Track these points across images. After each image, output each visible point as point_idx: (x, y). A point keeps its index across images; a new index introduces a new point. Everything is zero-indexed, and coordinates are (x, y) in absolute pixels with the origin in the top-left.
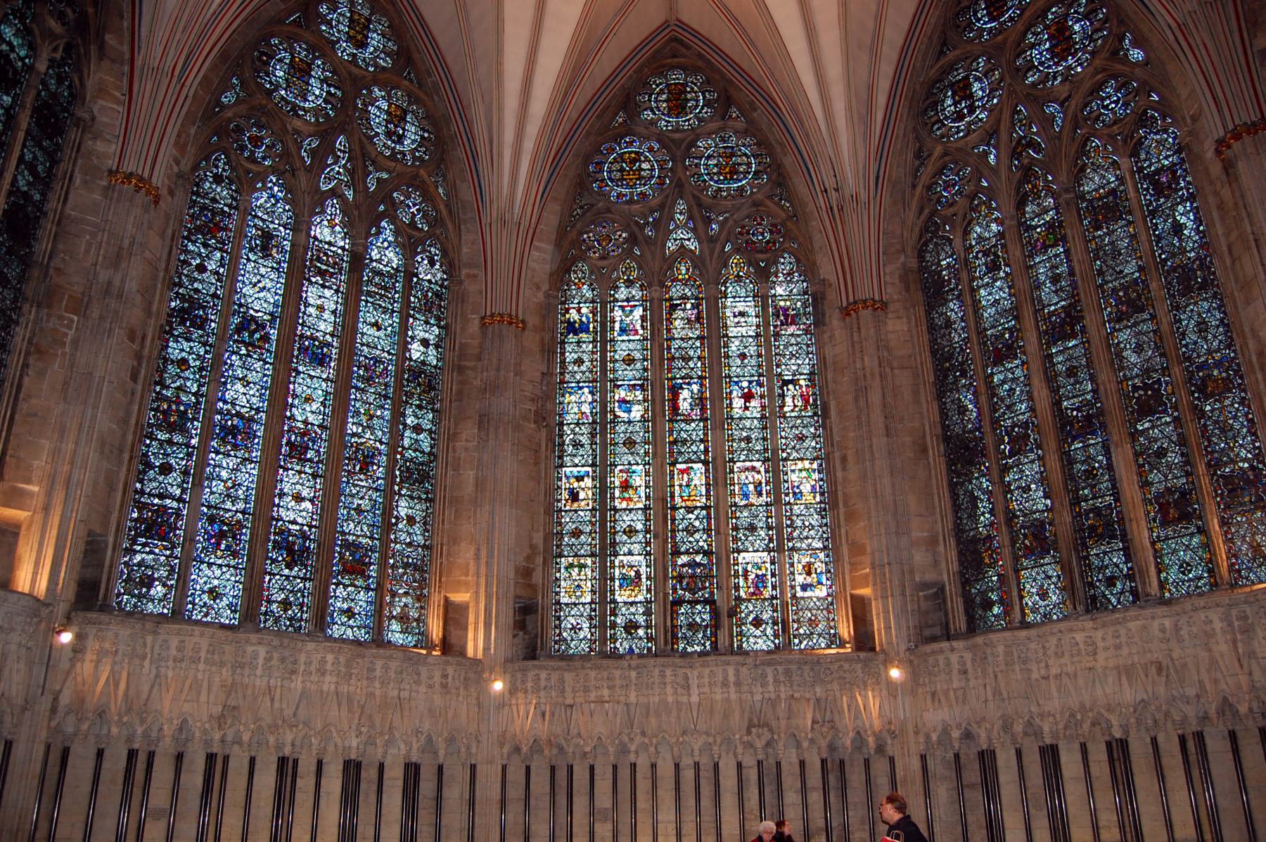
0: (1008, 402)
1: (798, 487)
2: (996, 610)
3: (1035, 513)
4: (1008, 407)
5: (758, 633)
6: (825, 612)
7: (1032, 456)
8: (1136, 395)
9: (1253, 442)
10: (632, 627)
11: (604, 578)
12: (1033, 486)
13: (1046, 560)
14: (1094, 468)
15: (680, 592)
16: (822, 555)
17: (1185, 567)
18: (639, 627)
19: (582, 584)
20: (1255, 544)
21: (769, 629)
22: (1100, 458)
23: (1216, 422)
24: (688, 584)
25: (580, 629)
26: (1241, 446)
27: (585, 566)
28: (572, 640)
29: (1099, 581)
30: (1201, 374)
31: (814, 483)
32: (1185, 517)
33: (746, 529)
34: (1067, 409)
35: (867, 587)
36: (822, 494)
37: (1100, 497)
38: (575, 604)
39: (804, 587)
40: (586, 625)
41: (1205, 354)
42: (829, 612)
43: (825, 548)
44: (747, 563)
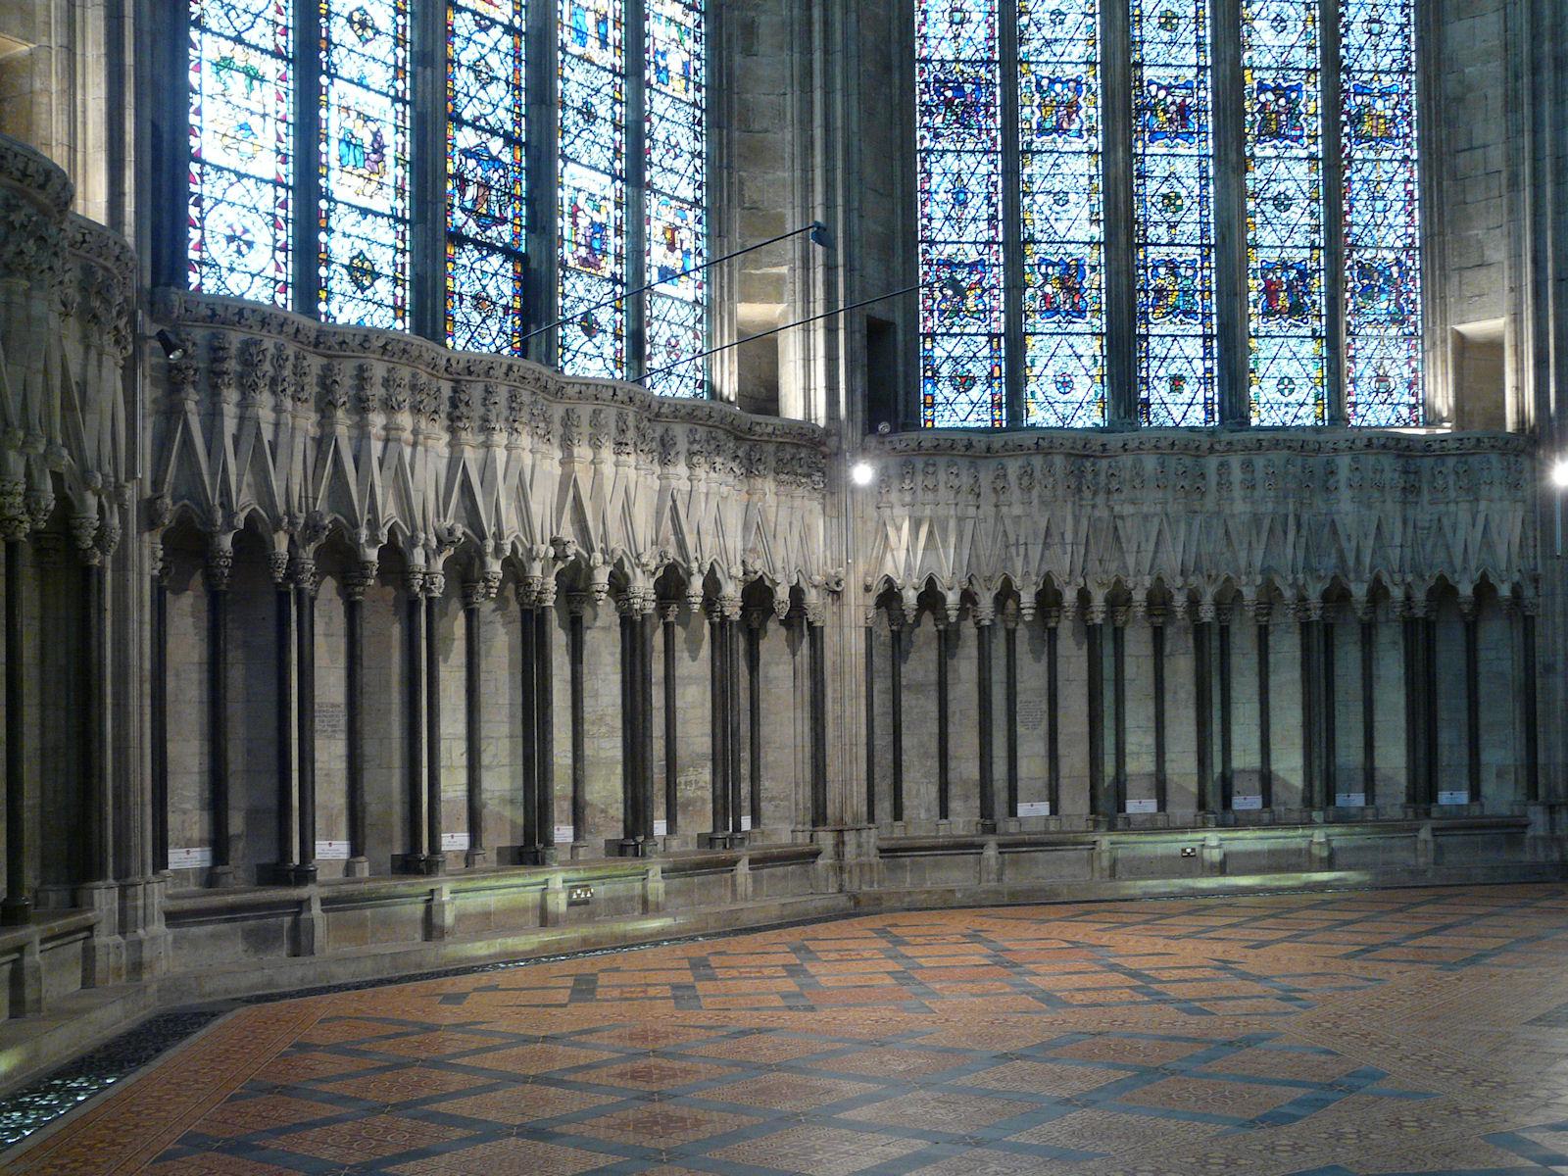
0: (1047, 32)
1: (663, 55)
2: (975, 393)
3: (1069, 242)
4: (1048, 43)
5: (589, 348)
6: (690, 334)
7: (1077, 145)
8: (1262, 98)
9: (1408, 225)
10: (365, 272)
11: (307, 129)
12: (1072, 197)
13: (1076, 328)
14: (1178, 196)
15: (458, 214)
16: (690, 215)
17: (1286, 384)
18: (376, 276)
19: (255, 122)
20: (1381, 372)
21: (607, 344)
22: (1191, 182)
23: (1366, 181)
24: (475, 201)
25: (250, 244)
26: (1390, 226)
27: (253, 76)
28: (232, 270)
29: (1160, 379)
30: (1359, 99)
31: (686, 57)
32: (1297, 310)
33: (579, 112)
34: (1150, 83)
35: (780, 301)
36: (698, 89)
37: (1179, 245)
38: (240, 176)
39: (666, 275)
40: (262, 236)
41: (1370, 72)
42: (696, 337)
43: (696, 203)
44: (579, 190)
